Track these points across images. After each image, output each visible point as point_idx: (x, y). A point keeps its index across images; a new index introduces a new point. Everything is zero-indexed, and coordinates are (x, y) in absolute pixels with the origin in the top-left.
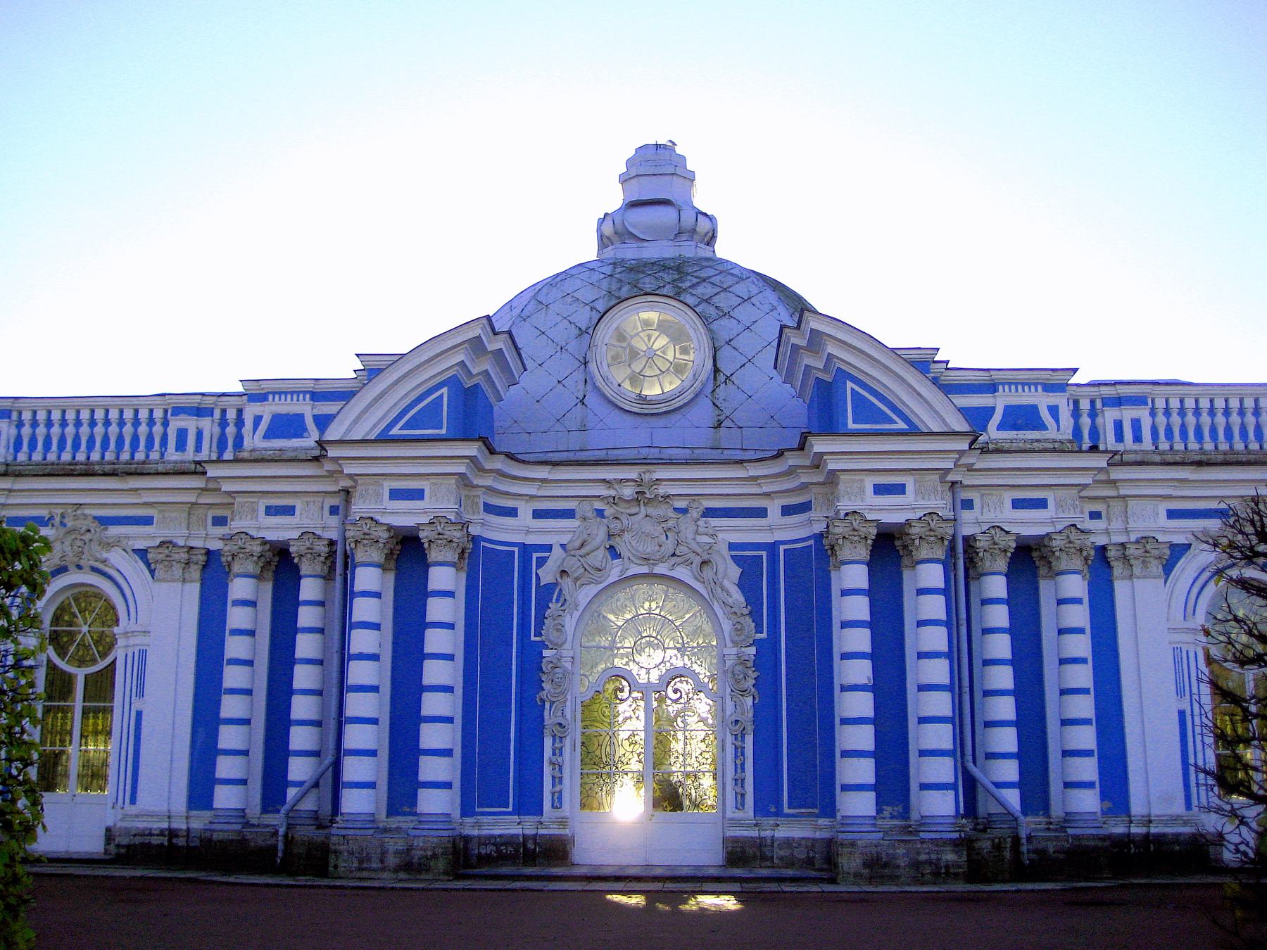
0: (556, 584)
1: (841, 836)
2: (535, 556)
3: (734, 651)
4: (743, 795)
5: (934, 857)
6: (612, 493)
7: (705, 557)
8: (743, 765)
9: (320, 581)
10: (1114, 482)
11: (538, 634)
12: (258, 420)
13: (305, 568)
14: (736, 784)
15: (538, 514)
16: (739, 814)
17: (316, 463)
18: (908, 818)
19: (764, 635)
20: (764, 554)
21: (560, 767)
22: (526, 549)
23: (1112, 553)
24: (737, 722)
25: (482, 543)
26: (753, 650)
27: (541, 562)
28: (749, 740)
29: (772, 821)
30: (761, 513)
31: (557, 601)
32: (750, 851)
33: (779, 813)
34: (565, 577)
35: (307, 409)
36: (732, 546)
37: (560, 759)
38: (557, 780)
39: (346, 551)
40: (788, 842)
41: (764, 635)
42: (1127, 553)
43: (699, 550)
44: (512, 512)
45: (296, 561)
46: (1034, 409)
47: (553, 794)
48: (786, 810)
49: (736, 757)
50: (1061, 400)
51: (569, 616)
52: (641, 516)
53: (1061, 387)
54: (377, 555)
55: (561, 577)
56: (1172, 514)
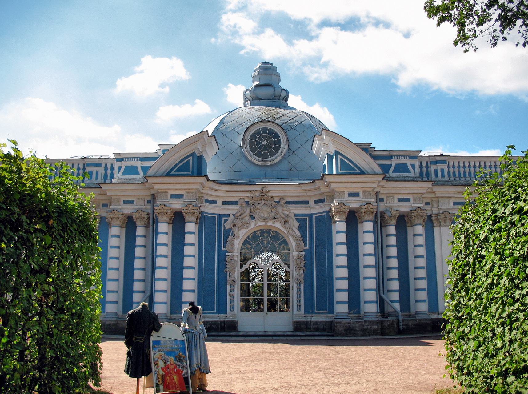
0: (231, 229)
1: (336, 320)
2: (223, 219)
3: (297, 253)
4: (300, 306)
5: (369, 327)
6: (252, 195)
7: (286, 219)
8: (300, 295)
9: (144, 228)
10: (434, 192)
11: (225, 247)
12: (120, 168)
13: (138, 224)
14: (297, 302)
15: (224, 203)
16: (298, 313)
17: (142, 184)
18: (360, 314)
19: (307, 247)
20: (307, 218)
21: (233, 296)
22: (220, 216)
23: (433, 218)
24: (298, 279)
25: (204, 214)
26: (303, 253)
27: (226, 221)
28: (302, 286)
29: (310, 315)
30: (306, 203)
31: (232, 235)
32: (303, 326)
33: (313, 312)
34: (235, 227)
35: (139, 164)
36: (296, 215)
37: (233, 293)
38: (232, 301)
39: (154, 217)
40: (316, 323)
41: (307, 247)
42: (439, 217)
43: (284, 217)
44: (215, 202)
45: (135, 220)
46: (405, 165)
47: (231, 306)
48: (316, 311)
49: (297, 292)
50: (415, 162)
51: (236, 240)
52: (262, 204)
53: (415, 157)
54: (166, 219)
55: (233, 226)
56: (455, 203)
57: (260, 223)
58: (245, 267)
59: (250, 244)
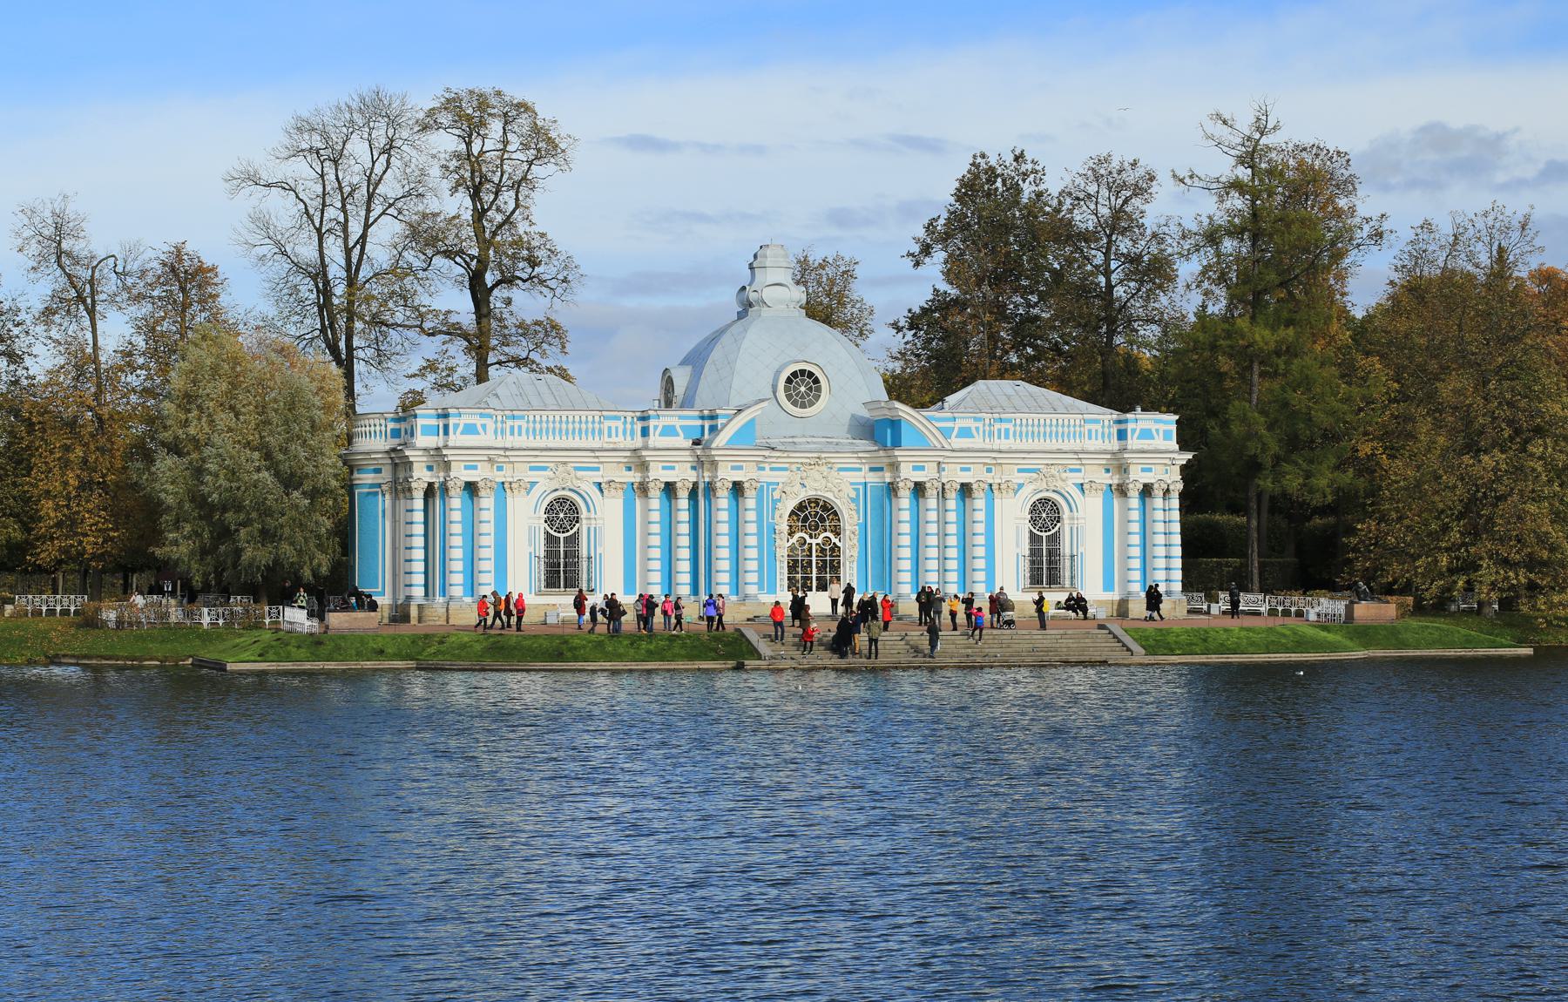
20: (861, 487)
27: (774, 490)
28: (855, 563)
56: (1020, 471)
57: (811, 493)
58: (791, 541)
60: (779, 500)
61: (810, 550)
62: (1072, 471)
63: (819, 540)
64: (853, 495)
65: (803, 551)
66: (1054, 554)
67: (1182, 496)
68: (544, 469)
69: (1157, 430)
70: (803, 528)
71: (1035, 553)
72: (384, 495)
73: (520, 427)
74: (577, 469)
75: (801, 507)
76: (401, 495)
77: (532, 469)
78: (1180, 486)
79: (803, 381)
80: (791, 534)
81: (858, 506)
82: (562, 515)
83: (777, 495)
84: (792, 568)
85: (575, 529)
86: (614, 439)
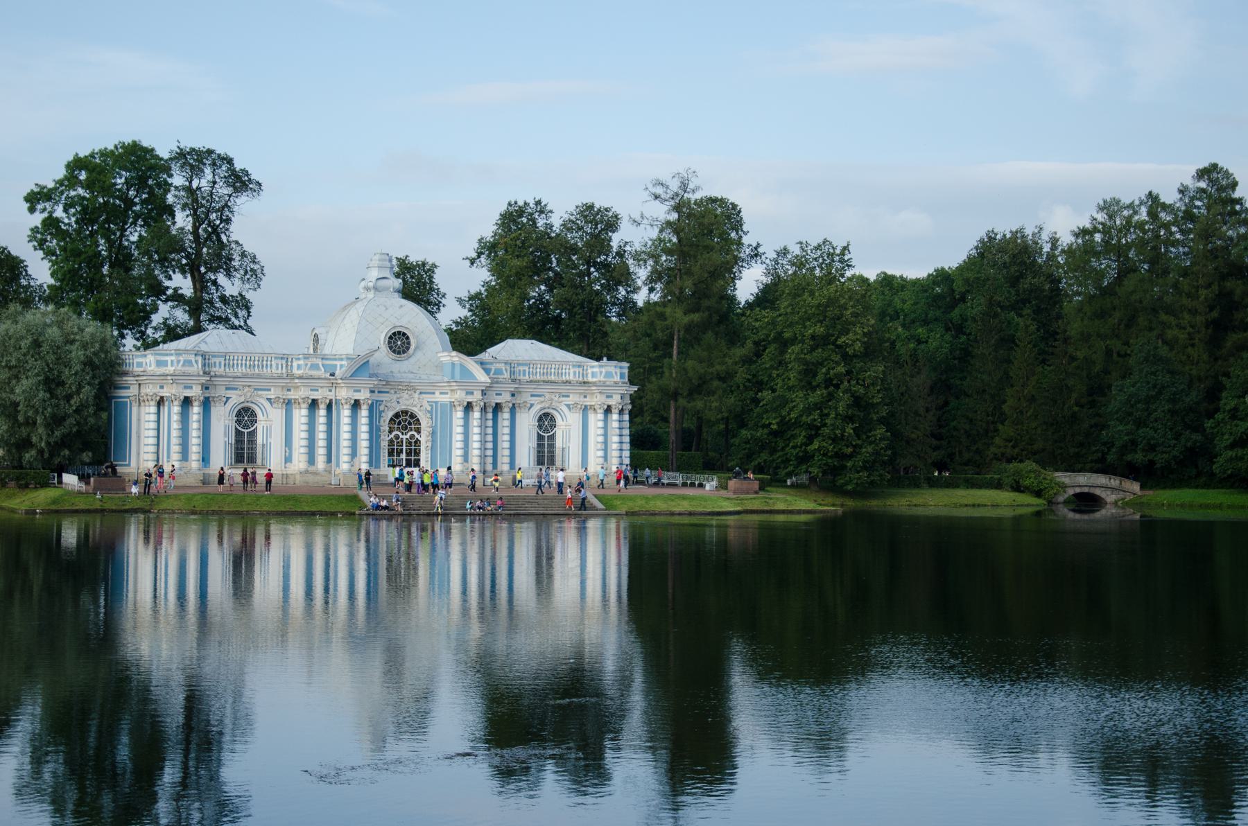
27: (380, 405)
28: (429, 451)
30: (434, 393)
57: (404, 408)
59: (395, 421)
60: (383, 411)
61: (402, 442)
62: (563, 396)
63: (408, 436)
64: (429, 408)
65: (398, 442)
66: (552, 446)
67: (630, 413)
68: (236, 389)
69: (616, 373)
70: (398, 429)
71: (540, 446)
72: (131, 404)
73: (220, 363)
74: (255, 389)
75: (397, 415)
76: (142, 404)
77: (227, 389)
78: (630, 407)
79: (399, 338)
80: (390, 432)
81: (432, 415)
82: (246, 418)
83: (382, 408)
84: (391, 453)
85: (254, 427)
86: (279, 371)
